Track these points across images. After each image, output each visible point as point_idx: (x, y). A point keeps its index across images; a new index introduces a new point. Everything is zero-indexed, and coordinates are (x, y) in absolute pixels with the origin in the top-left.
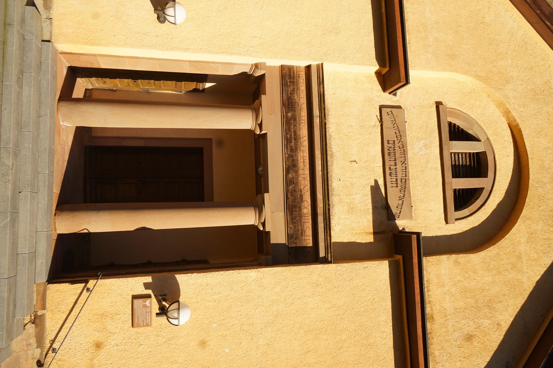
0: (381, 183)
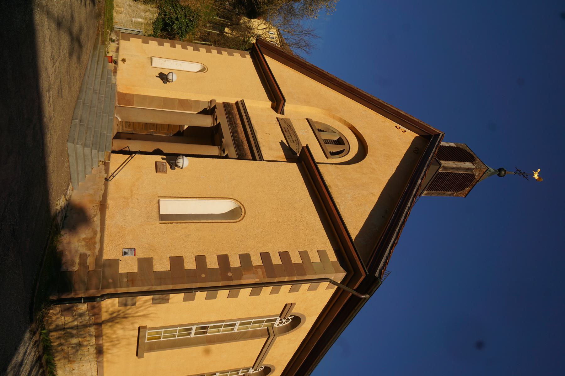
0: (285, 141)
